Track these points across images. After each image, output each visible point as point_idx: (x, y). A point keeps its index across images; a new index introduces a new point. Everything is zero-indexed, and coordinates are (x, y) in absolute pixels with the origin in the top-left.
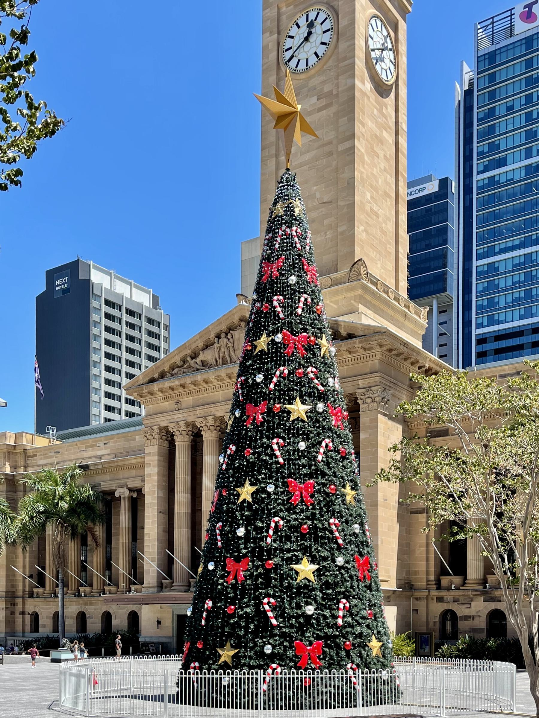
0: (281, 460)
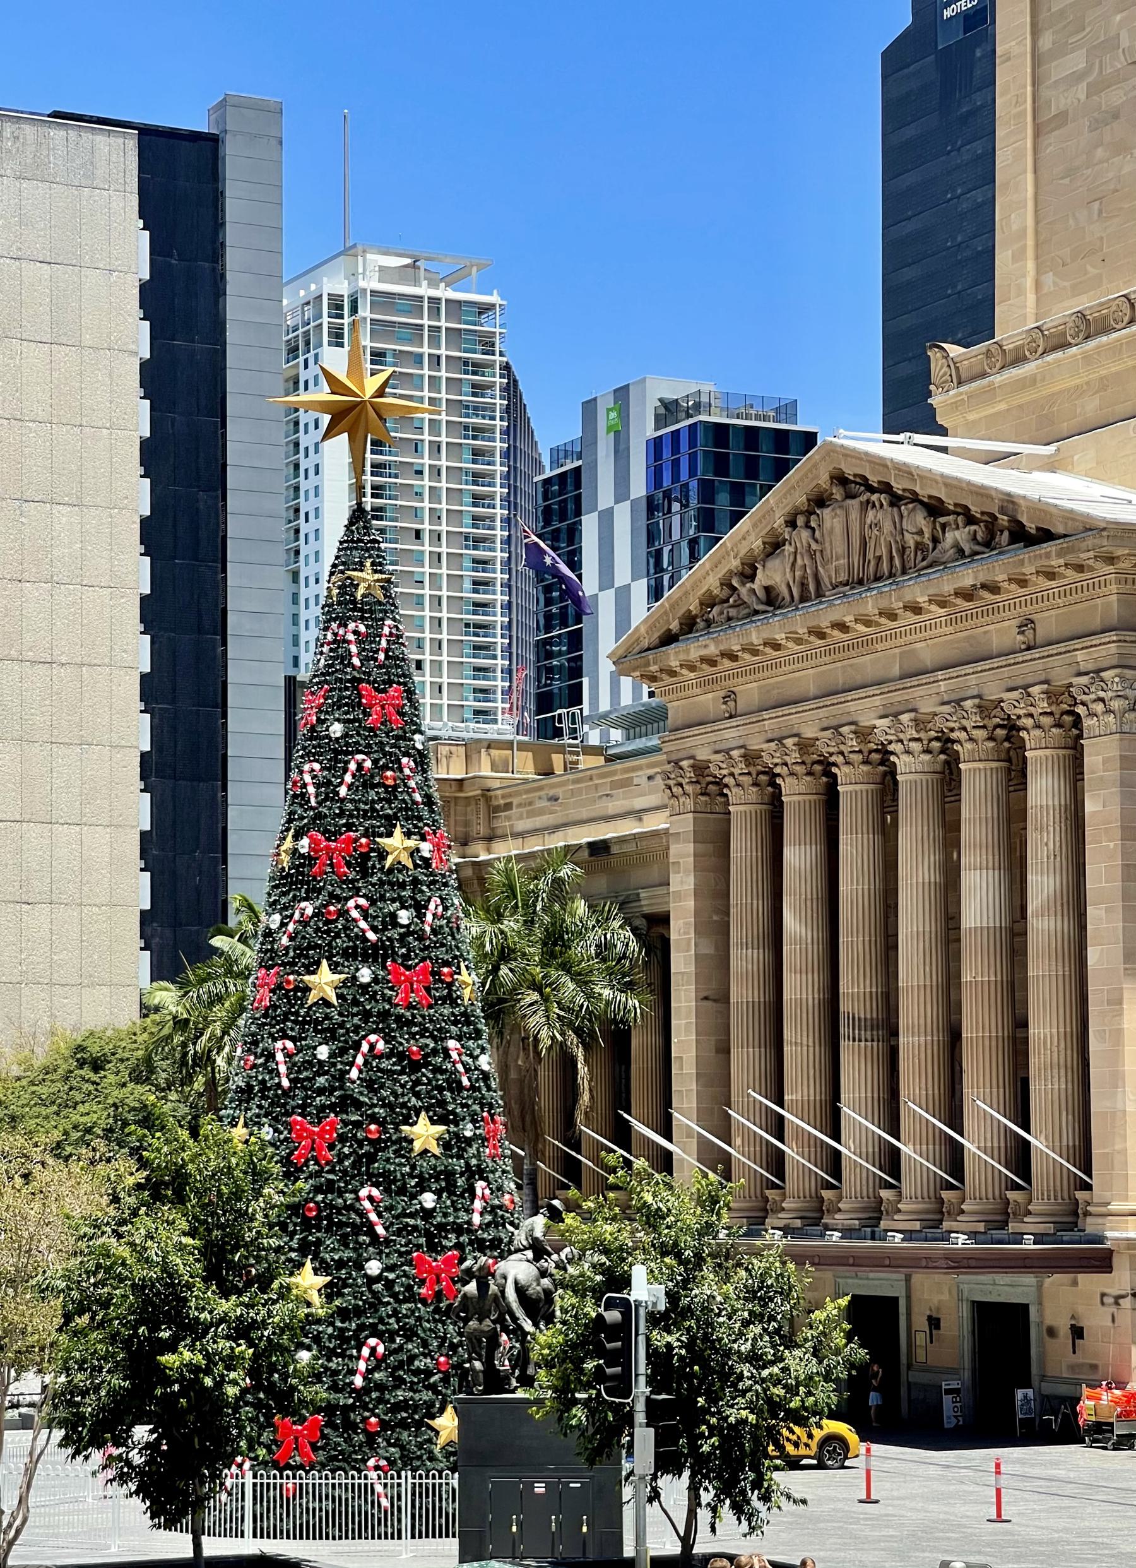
0: (286, 1083)
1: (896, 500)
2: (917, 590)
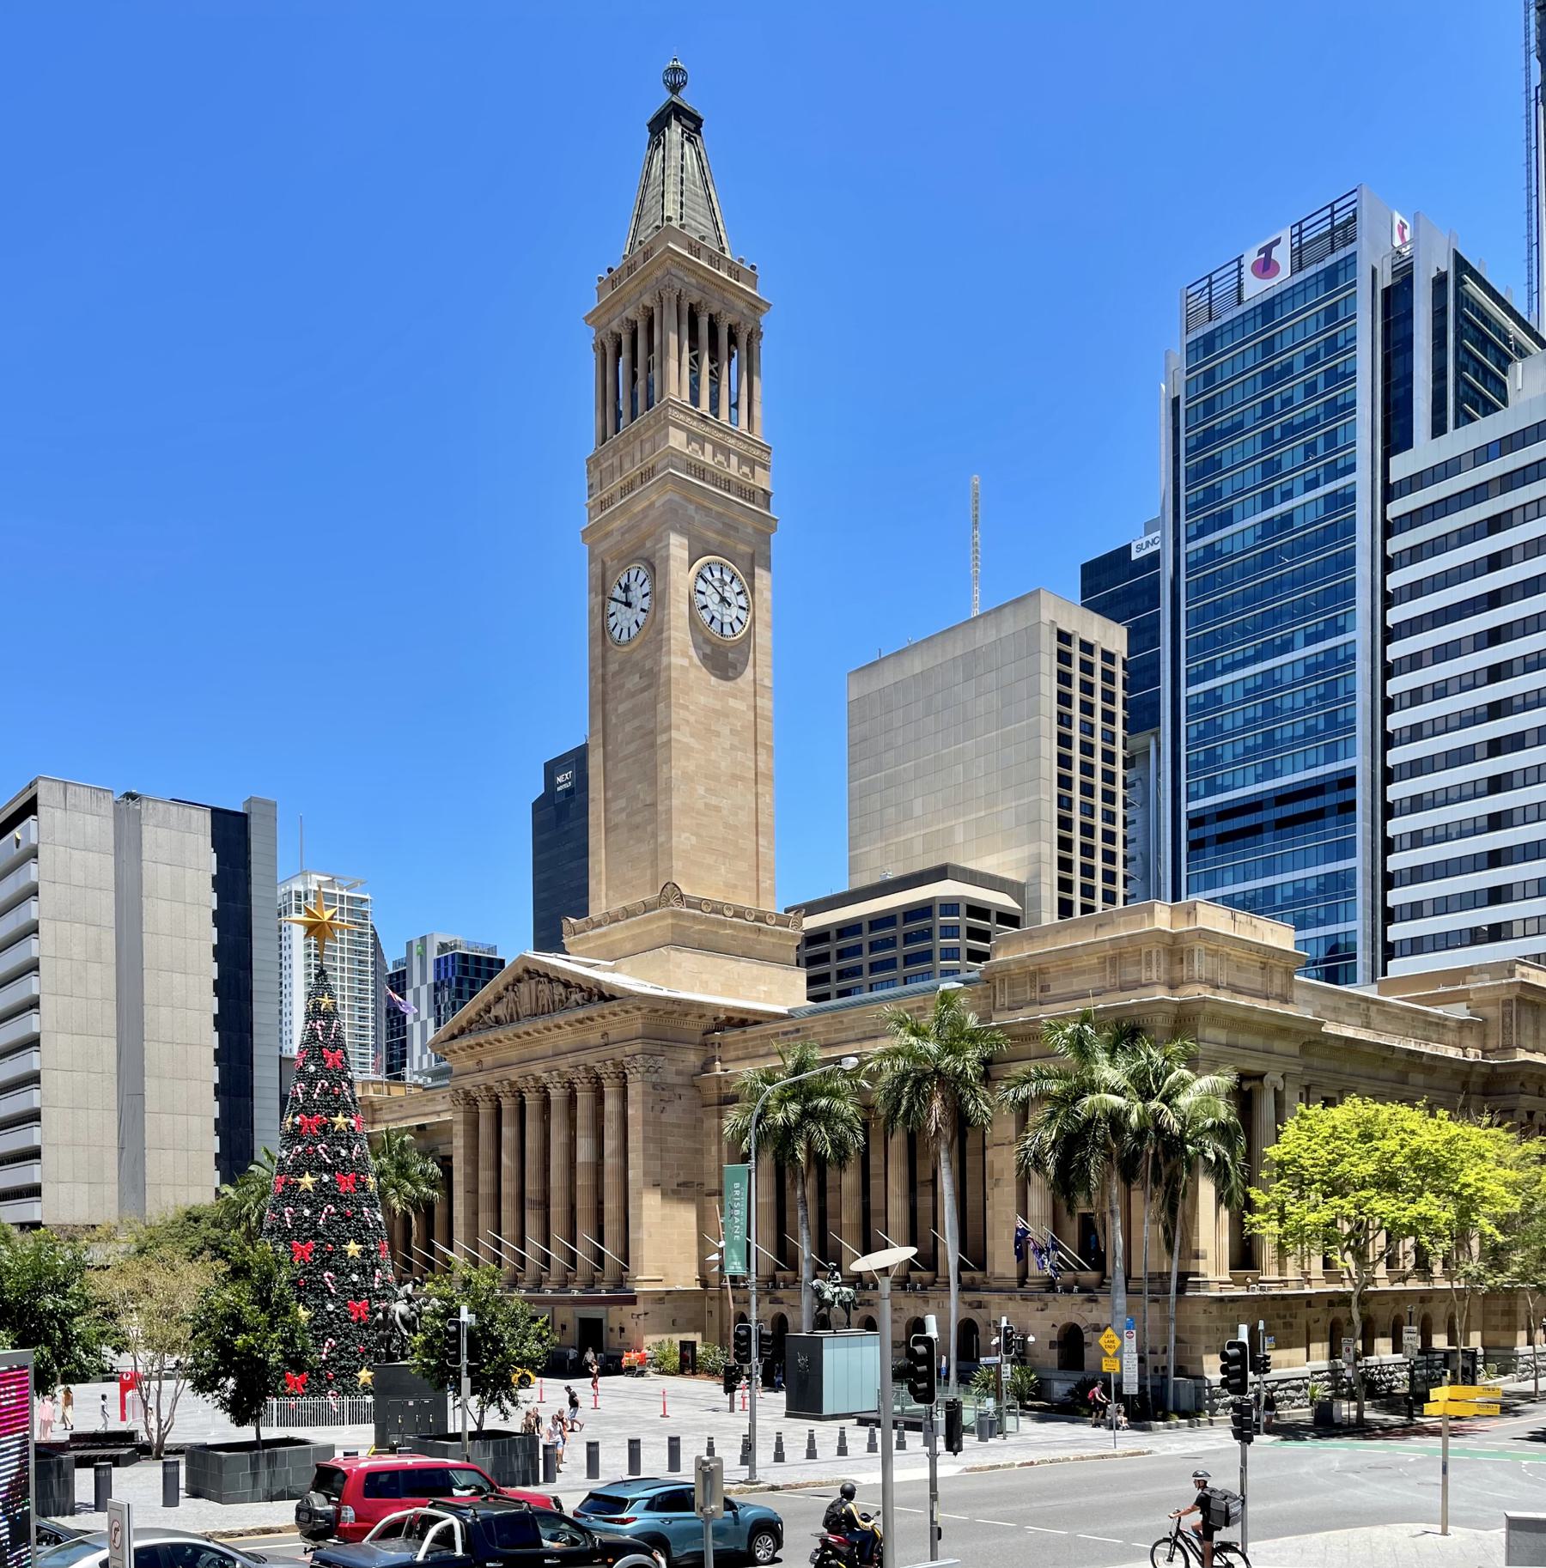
1: (551, 981)
2: (560, 1019)
